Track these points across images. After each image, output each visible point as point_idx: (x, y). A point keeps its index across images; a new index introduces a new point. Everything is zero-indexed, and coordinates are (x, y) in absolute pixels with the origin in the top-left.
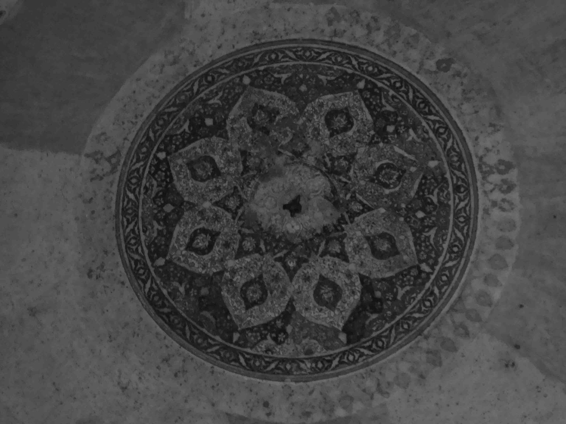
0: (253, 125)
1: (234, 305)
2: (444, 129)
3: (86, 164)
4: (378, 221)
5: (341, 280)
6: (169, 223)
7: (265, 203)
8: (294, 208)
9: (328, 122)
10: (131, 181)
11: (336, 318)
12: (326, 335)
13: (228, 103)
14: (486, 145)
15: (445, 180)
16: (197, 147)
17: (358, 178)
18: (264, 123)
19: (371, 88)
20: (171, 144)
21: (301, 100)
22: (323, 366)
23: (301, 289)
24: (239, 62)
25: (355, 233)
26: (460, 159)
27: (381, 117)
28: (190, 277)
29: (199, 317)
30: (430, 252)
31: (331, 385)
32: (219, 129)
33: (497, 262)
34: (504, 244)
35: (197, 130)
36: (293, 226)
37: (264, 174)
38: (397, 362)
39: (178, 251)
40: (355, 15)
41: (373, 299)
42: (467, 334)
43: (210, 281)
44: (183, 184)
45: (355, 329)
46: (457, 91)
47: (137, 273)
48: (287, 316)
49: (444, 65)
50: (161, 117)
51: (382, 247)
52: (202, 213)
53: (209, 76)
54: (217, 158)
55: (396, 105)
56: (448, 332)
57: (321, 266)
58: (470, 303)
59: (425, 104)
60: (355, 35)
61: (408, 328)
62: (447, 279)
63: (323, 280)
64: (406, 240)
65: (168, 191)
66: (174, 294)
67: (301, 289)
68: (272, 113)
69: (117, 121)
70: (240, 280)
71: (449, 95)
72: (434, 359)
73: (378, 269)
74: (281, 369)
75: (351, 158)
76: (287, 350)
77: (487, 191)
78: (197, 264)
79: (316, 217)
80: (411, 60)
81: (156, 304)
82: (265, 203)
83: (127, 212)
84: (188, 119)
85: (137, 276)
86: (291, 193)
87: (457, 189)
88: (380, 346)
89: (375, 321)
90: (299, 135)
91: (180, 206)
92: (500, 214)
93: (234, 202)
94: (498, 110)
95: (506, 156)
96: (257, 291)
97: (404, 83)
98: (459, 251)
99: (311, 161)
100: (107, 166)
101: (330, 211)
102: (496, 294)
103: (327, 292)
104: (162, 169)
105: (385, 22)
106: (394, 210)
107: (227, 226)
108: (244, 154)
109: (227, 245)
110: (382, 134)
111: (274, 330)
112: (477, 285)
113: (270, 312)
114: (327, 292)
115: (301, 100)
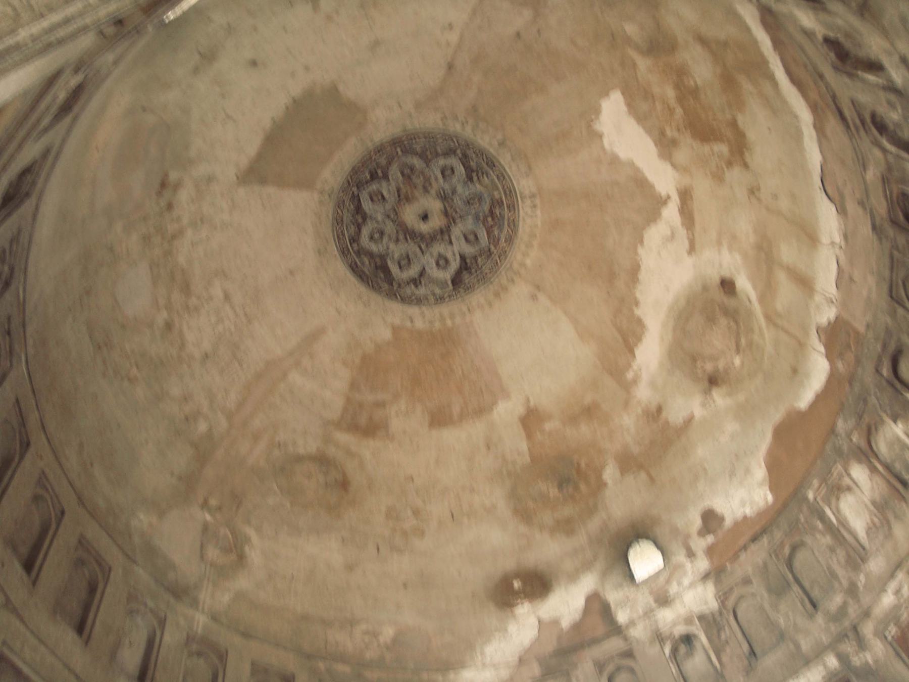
0: (403, 174)
1: (394, 269)
2: (502, 176)
3: (316, 196)
4: (469, 224)
5: (449, 255)
6: (359, 227)
7: (410, 215)
8: (425, 217)
9: (443, 173)
10: (340, 204)
11: (446, 275)
12: (443, 284)
13: (389, 163)
14: (523, 185)
15: (502, 202)
16: (374, 187)
17: (458, 202)
18: (408, 174)
19: (465, 156)
20: (360, 185)
21: (427, 162)
22: (440, 300)
23: (429, 261)
24: (396, 142)
25: (457, 231)
26: (510, 192)
27: (469, 171)
28: (371, 255)
29: (375, 274)
30: (495, 241)
31: (445, 309)
32: (386, 177)
33: (529, 245)
34: (533, 236)
35: (374, 176)
36: (424, 228)
37: (408, 199)
38: (478, 297)
39: (365, 240)
40: (456, 118)
41: (465, 265)
42: (513, 281)
43: (383, 257)
44: (367, 205)
45: (457, 281)
46: (508, 156)
47: (344, 252)
48: (422, 273)
49: (502, 144)
50: (355, 171)
51: (471, 238)
52: (377, 222)
53: (380, 149)
54: (385, 193)
55: (477, 164)
56: (504, 281)
57: (439, 248)
58: (515, 266)
59: (492, 164)
60: (455, 127)
61: (484, 279)
62: (503, 254)
63: (440, 256)
64: (483, 234)
65: (359, 209)
66: (363, 264)
67: (429, 261)
68: (412, 169)
69: (333, 174)
70: (396, 256)
71: (505, 159)
72: (497, 295)
73: (469, 250)
74: (419, 301)
75: (454, 192)
76: (422, 291)
77: (524, 209)
78: (374, 248)
79: (436, 222)
80: (485, 141)
81: (354, 269)
82: (410, 215)
83: (338, 221)
84: (369, 173)
85: (343, 253)
86: (423, 209)
87: (509, 207)
88: (469, 289)
89: (466, 276)
90: (427, 180)
91: (365, 218)
92: (530, 219)
93: (394, 216)
94: (530, 167)
95: (534, 190)
96: (406, 261)
97: (481, 153)
98: (510, 240)
99: (433, 192)
100: (327, 197)
101: (442, 217)
102: (528, 262)
103: (442, 262)
104: (356, 199)
105: (471, 121)
106: (477, 218)
107: (390, 228)
108: (398, 190)
109: (390, 238)
110: (470, 179)
111: (416, 282)
112: (519, 257)
113: (413, 272)
114: (442, 262)
115: (427, 162)
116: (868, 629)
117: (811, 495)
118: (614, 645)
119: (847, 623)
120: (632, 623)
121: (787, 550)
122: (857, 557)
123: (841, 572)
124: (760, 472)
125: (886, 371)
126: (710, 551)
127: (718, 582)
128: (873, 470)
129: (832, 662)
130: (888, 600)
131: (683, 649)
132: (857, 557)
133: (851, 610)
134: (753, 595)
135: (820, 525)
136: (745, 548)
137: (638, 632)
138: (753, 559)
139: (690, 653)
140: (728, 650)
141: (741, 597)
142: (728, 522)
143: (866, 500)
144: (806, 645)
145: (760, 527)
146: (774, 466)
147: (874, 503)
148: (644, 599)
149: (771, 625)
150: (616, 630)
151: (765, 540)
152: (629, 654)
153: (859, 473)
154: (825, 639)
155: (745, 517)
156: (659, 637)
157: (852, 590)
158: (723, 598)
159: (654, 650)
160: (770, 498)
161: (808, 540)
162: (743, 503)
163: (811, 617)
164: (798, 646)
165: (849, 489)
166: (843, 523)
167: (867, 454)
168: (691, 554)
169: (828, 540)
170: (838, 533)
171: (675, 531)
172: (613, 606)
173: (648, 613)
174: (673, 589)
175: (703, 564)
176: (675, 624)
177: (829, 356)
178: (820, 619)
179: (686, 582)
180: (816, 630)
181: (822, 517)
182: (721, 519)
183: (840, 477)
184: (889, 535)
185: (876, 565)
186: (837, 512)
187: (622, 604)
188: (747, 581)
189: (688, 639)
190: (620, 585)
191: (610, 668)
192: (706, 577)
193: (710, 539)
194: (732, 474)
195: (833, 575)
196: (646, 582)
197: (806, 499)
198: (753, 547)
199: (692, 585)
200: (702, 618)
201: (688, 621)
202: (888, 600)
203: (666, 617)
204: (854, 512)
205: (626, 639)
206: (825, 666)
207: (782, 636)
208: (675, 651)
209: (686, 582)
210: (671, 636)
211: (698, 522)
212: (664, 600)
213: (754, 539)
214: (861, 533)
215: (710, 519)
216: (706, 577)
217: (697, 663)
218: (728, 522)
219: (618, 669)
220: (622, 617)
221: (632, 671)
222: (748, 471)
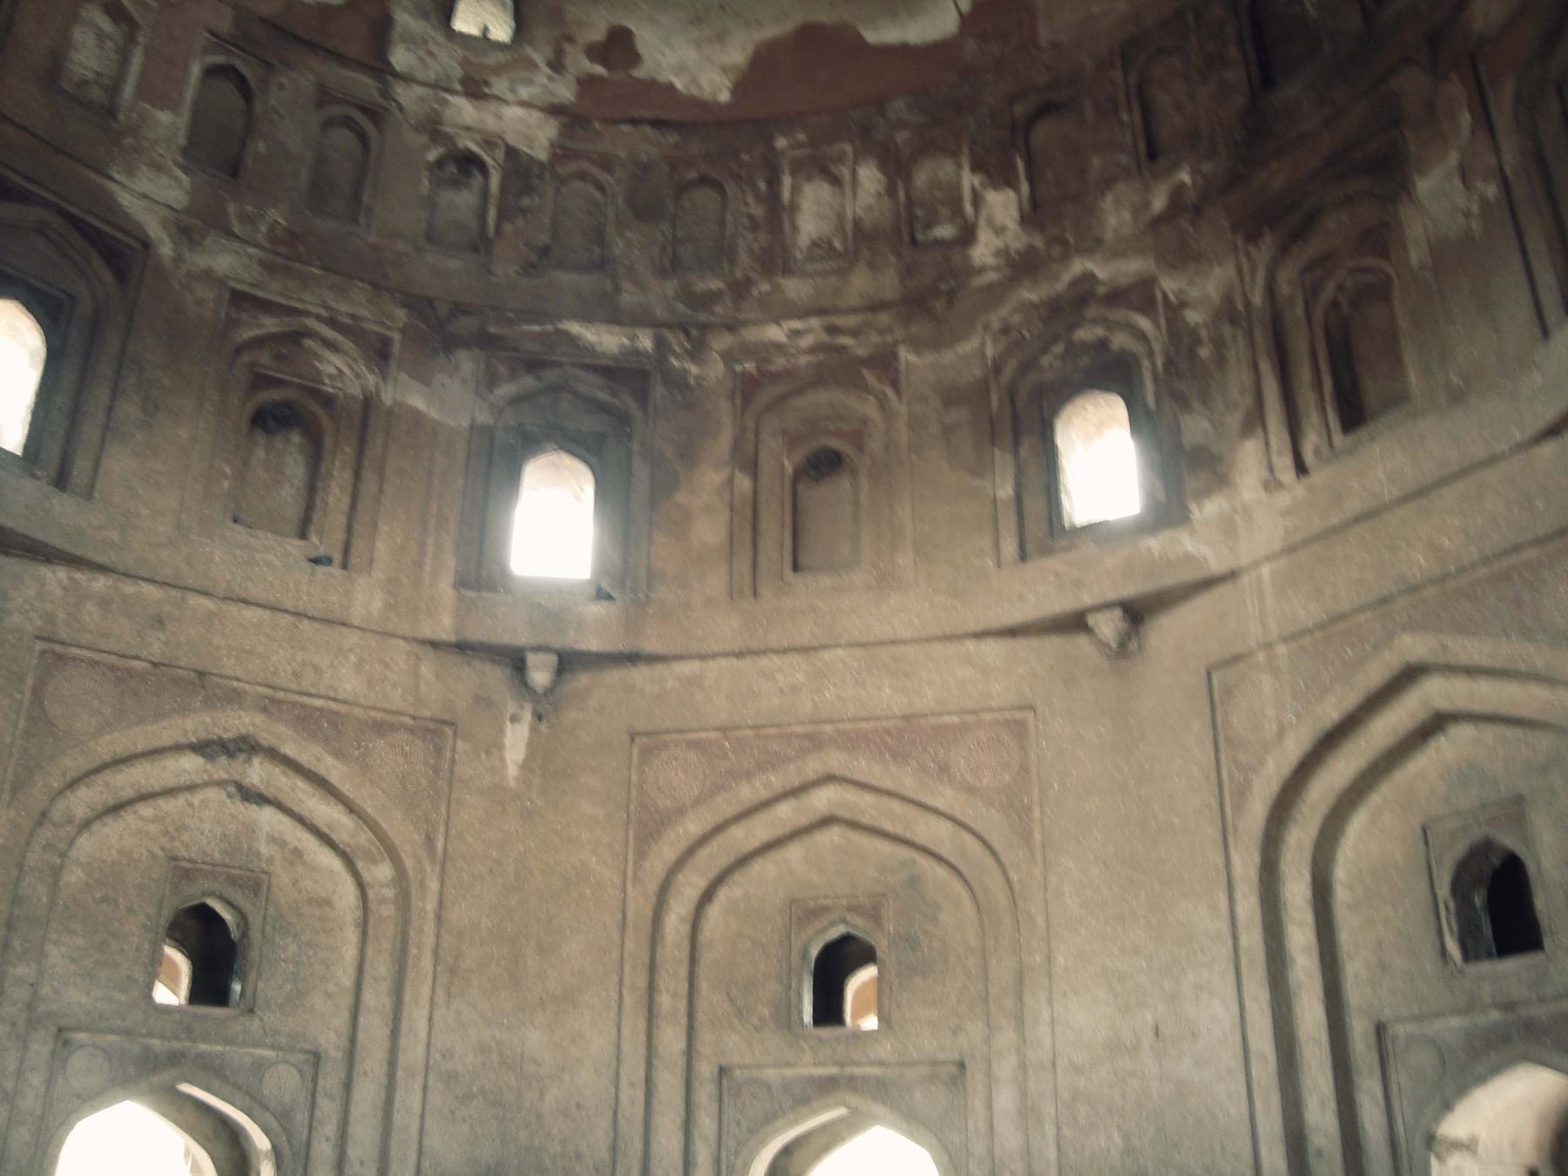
116: (721, 342)
117: (781, 143)
118: (365, 85)
119: (702, 317)
120: (407, 79)
121: (692, 175)
122: (776, 260)
123: (743, 258)
124: (737, 55)
125: (1019, 110)
126: (586, 84)
127: (567, 131)
128: (891, 191)
129: (646, 342)
130: (775, 333)
131: (452, 168)
132: (776, 260)
133: (719, 309)
134: (601, 188)
135: (762, 186)
136: (634, 122)
137: (407, 96)
138: (631, 144)
139: (456, 184)
140: (520, 222)
141: (582, 176)
142: (640, 73)
143: (849, 214)
144: (629, 297)
145: (679, 117)
146: (764, 64)
147: (857, 223)
148: (447, 62)
149: (600, 238)
150: (381, 69)
151: (672, 138)
152: (376, 115)
153: (870, 177)
154: (659, 312)
155: (671, 87)
156: (433, 128)
157: (740, 289)
158: (561, 153)
159: (415, 139)
160: (724, 97)
161: (731, 188)
162: (681, 69)
163: (662, 273)
164: (617, 289)
165: (835, 181)
166: (794, 207)
167: (896, 167)
168: (557, 65)
169: (758, 211)
170: (778, 214)
171: (557, 16)
172: (396, 33)
173: (439, 86)
174: (499, 86)
175: (565, 92)
176: (468, 129)
177: (965, 21)
178: (670, 286)
179: (524, 92)
180: (660, 294)
181: (774, 182)
182: (634, 58)
183: (840, 159)
184: (843, 273)
185: (795, 288)
186: (795, 190)
187: (413, 42)
188: (606, 164)
189: (468, 163)
190: (425, 16)
191: (336, 110)
192: (555, 110)
193: (599, 70)
194: (697, 21)
195: (729, 254)
196: (465, 39)
197: (770, 140)
198: (649, 131)
199: (524, 104)
200: (512, 152)
201: (489, 143)
202: (775, 333)
203: (463, 110)
204: (814, 211)
205: (386, 94)
206: (633, 338)
207: (603, 264)
208: (440, 163)
209: (524, 92)
210: (447, 139)
211: (598, 35)
212: (475, 89)
213: (658, 124)
214: (803, 241)
215: (618, 48)
216: (555, 110)
217: (462, 201)
218: (640, 73)
219: (348, 122)
220: (400, 58)
221: (363, 139)
222: (721, 38)
